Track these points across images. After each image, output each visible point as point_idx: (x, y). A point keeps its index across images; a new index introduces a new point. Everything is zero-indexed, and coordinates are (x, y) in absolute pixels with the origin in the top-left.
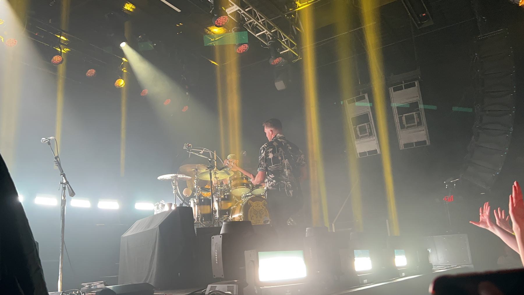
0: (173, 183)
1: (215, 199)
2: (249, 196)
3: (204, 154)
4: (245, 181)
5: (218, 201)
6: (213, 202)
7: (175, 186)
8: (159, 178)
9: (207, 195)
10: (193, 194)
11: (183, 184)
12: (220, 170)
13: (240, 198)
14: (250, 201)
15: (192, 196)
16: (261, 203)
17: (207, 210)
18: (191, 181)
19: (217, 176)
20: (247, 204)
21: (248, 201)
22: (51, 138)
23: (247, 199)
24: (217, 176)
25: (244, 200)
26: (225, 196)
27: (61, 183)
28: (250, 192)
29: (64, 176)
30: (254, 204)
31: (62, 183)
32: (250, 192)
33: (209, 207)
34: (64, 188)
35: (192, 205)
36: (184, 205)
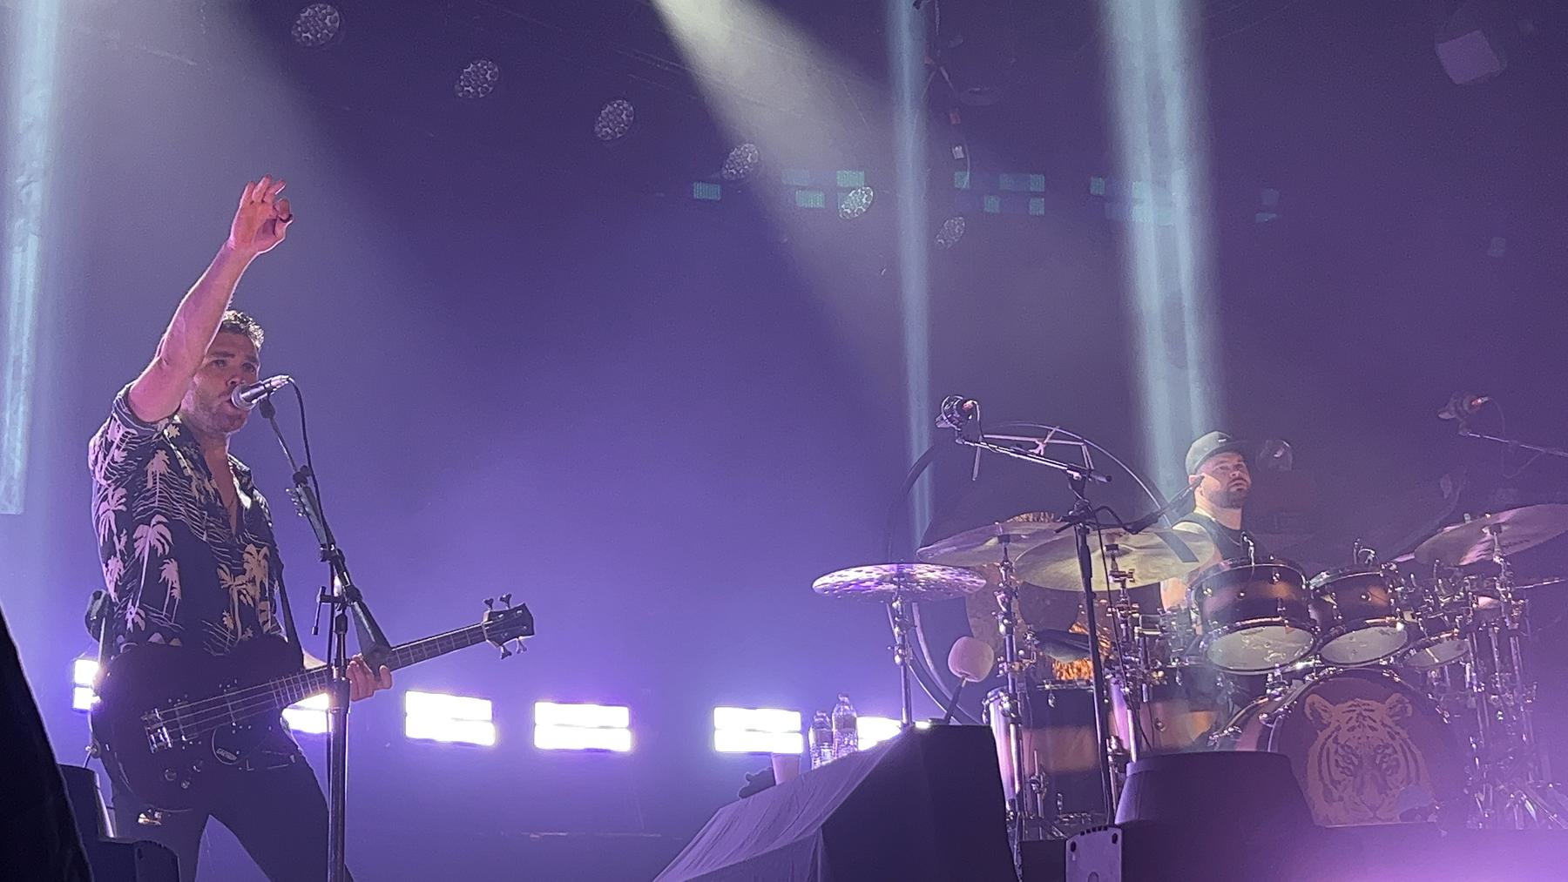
0: (895, 612)
1: (1118, 692)
2: (1307, 671)
3: (1050, 452)
4: (1281, 590)
5: (1132, 702)
6: (1106, 710)
7: (906, 626)
8: (817, 583)
9: (1075, 669)
10: (995, 669)
11: (946, 615)
12: (1137, 528)
13: (1254, 684)
14: (1314, 698)
15: (995, 681)
16: (1380, 710)
17: (1077, 751)
18: (987, 593)
19: (1124, 564)
20: (1297, 709)
21: (1301, 698)
22: (276, 381)
23: (1298, 687)
24: (1124, 564)
25: (1279, 698)
26: (1170, 673)
27: (324, 598)
28: (1313, 651)
29: (337, 563)
30: (1338, 714)
31: (331, 599)
32: (1313, 651)
33: (1085, 734)
34: (341, 624)
35: (997, 725)
36: (954, 722)
